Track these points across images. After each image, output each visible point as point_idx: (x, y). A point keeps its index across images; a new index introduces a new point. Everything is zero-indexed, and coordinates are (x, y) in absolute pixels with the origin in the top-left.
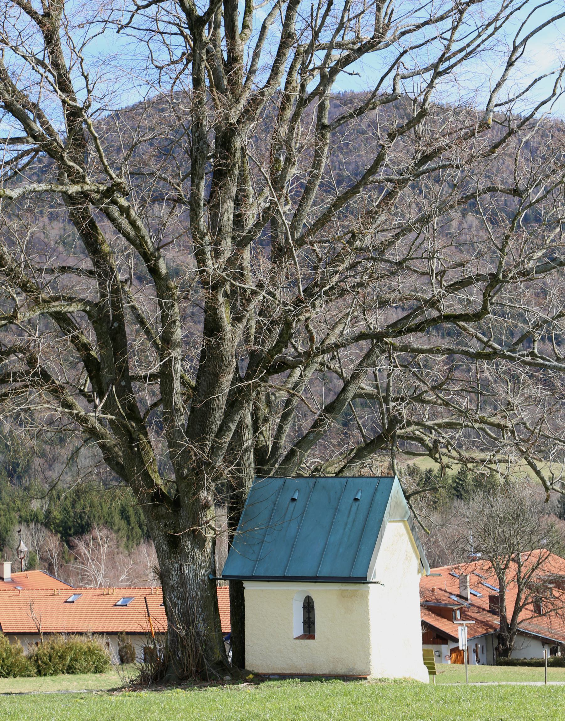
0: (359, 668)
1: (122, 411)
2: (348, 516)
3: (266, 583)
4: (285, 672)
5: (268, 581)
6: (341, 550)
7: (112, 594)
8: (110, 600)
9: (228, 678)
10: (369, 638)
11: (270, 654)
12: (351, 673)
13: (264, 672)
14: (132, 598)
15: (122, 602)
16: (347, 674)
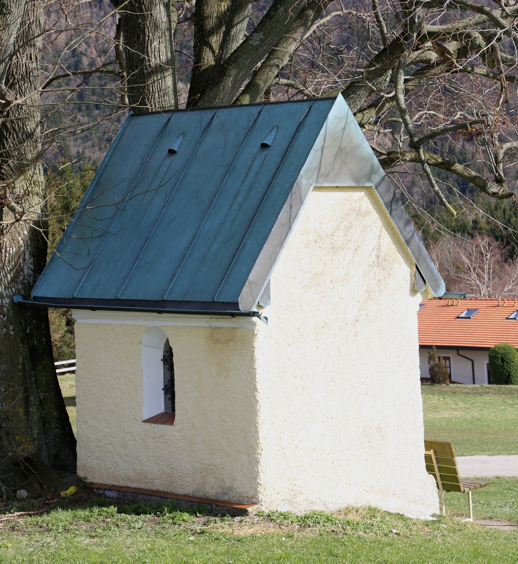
0: (240, 488)
1: (394, 119)
2: (244, 181)
3: (89, 312)
4: (130, 485)
5: (93, 309)
6: (215, 247)
7: (457, 305)
8: (453, 312)
9: (23, 493)
10: (256, 427)
11: (110, 447)
12: (226, 498)
13: (101, 481)
14: (477, 309)
15: (466, 314)
16: (220, 498)
